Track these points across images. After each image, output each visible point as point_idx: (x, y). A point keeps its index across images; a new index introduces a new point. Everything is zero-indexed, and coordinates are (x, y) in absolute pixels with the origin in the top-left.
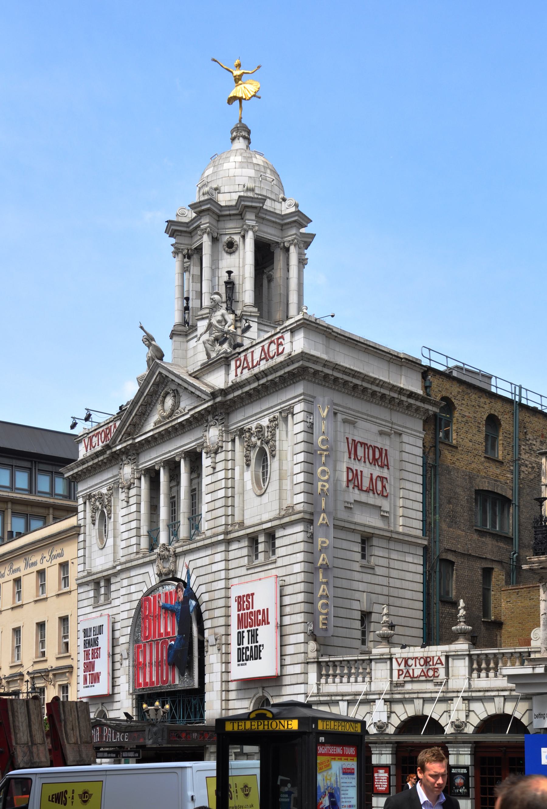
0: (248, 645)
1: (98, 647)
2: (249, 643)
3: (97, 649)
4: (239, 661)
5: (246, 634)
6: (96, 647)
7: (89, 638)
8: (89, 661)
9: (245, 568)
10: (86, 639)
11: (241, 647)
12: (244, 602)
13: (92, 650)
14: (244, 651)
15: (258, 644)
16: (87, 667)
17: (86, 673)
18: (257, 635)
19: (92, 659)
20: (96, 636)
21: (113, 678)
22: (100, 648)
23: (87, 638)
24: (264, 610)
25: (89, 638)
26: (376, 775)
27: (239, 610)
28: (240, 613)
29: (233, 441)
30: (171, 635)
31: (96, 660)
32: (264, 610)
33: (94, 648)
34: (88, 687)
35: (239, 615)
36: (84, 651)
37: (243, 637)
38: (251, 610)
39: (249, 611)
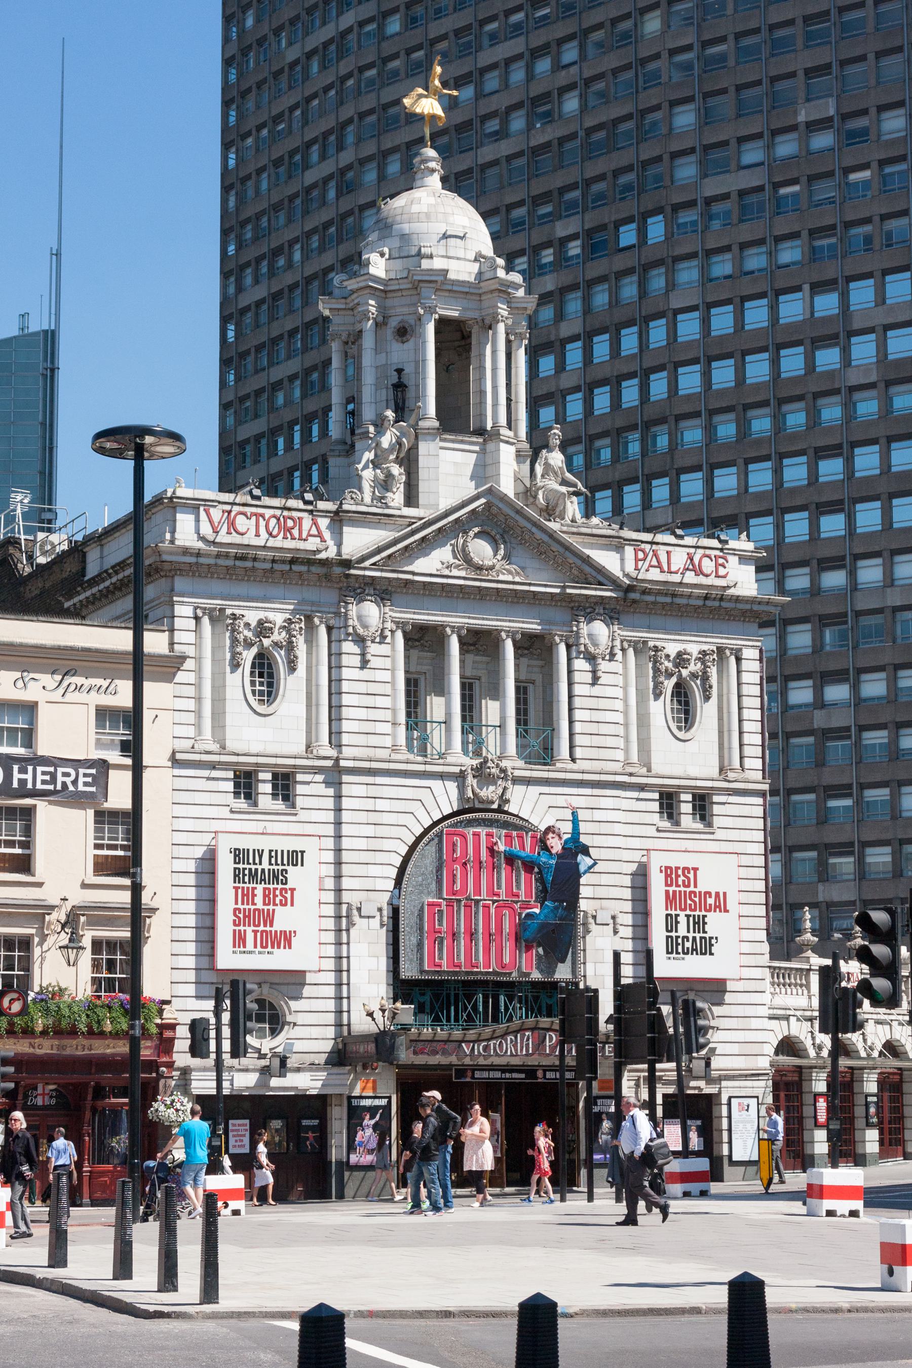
1: (287, 887)
2: (688, 931)
4: (668, 953)
5: (682, 919)
6: (280, 886)
7: (253, 867)
8: (253, 907)
9: (654, 828)
10: (241, 866)
11: (673, 934)
12: (677, 876)
14: (680, 941)
17: (242, 928)
18: (705, 923)
20: (281, 868)
22: (293, 890)
24: (717, 894)
27: (667, 885)
28: (671, 889)
31: (279, 909)
32: (717, 894)
33: (271, 886)
34: (250, 952)
35: (667, 892)
36: (236, 888)
38: (692, 888)
39: (688, 890)
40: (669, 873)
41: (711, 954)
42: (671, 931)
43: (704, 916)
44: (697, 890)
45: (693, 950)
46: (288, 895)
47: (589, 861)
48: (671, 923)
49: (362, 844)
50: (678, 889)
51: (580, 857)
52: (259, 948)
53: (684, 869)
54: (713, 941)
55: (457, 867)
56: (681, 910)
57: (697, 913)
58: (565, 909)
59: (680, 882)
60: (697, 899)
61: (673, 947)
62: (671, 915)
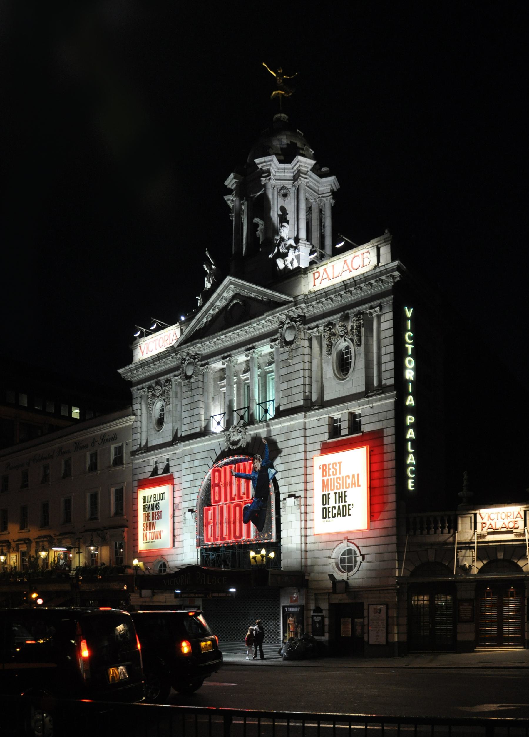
0: (334, 505)
2: (336, 503)
3: (158, 512)
4: (323, 518)
5: (332, 497)
6: (157, 511)
8: (149, 522)
10: (145, 504)
11: (327, 506)
12: (329, 469)
13: (153, 513)
14: (330, 510)
15: (347, 504)
16: (147, 526)
17: (146, 532)
18: (345, 496)
19: (153, 520)
20: (157, 502)
21: (174, 536)
22: (161, 511)
23: (147, 504)
24: (353, 476)
25: (149, 503)
26: (461, 607)
27: (323, 476)
28: (325, 479)
29: (310, 340)
30: (245, 499)
31: (157, 521)
32: (353, 476)
33: (154, 511)
35: (323, 481)
36: (144, 514)
37: (329, 498)
38: (338, 475)
39: (335, 477)
40: (324, 468)
41: (349, 515)
42: (325, 504)
43: (345, 492)
44: (341, 476)
45: (338, 514)
46: (160, 514)
47: (273, 471)
48: (325, 498)
49: (188, 485)
50: (329, 478)
51: (269, 470)
52: (151, 540)
53: (333, 464)
54: (351, 507)
55: (217, 489)
56: (331, 490)
57: (340, 491)
58: (262, 501)
59: (331, 473)
60: (341, 482)
61: (326, 514)
62: (325, 495)
